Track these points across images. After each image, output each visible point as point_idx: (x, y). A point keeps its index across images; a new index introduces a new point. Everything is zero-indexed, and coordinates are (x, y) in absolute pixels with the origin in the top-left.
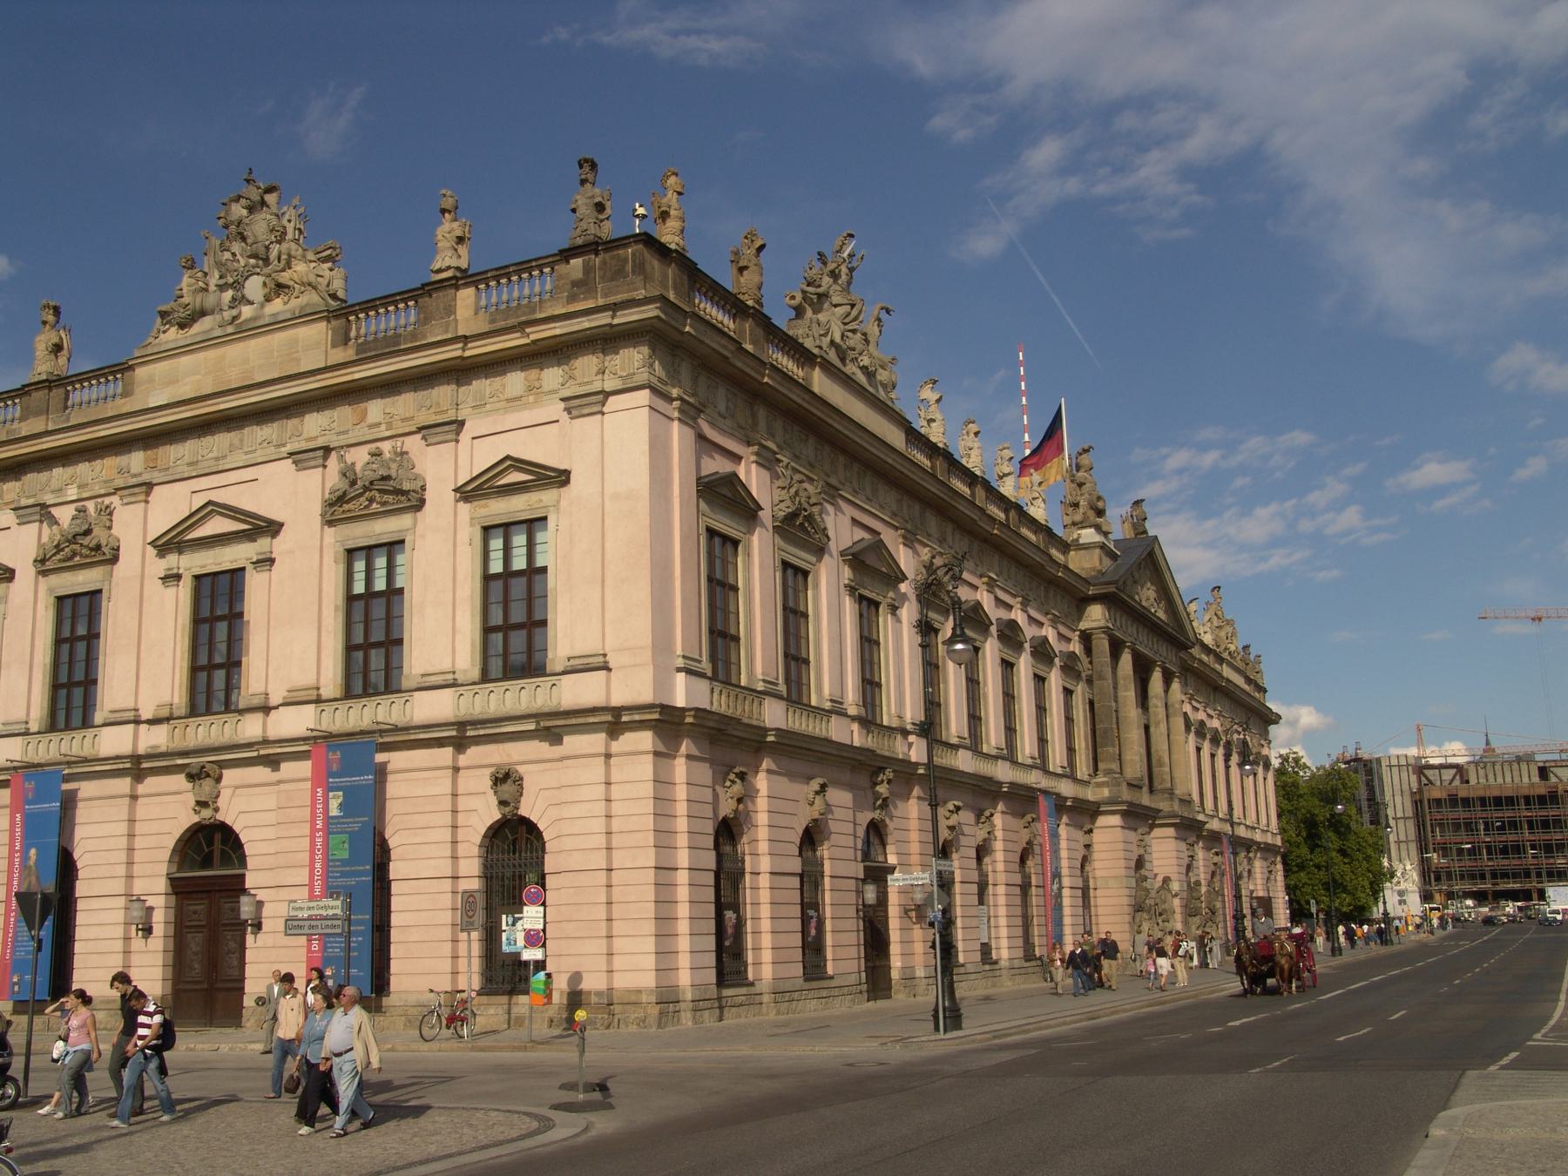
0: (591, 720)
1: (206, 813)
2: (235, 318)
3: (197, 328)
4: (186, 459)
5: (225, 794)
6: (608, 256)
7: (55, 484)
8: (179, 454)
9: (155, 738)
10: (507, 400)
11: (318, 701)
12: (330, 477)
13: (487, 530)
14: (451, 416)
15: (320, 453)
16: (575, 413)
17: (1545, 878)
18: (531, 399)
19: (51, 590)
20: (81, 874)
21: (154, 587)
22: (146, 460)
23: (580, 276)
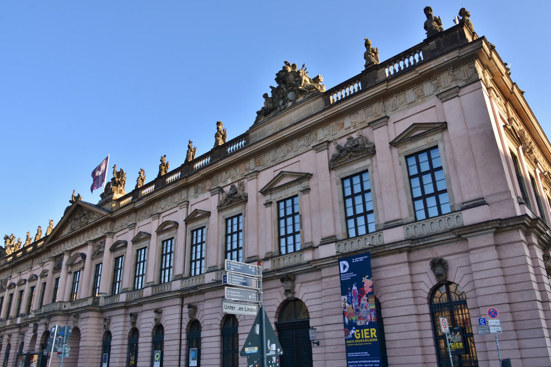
1: (290, 295)
2: (285, 107)
4: (271, 160)
5: (298, 286)
10: (408, 104)
11: (336, 241)
13: (407, 157)
14: (383, 115)
15: (326, 144)
18: (420, 100)
19: (223, 217)
20: (240, 324)
21: (262, 208)
22: (255, 163)
23: (435, 47)
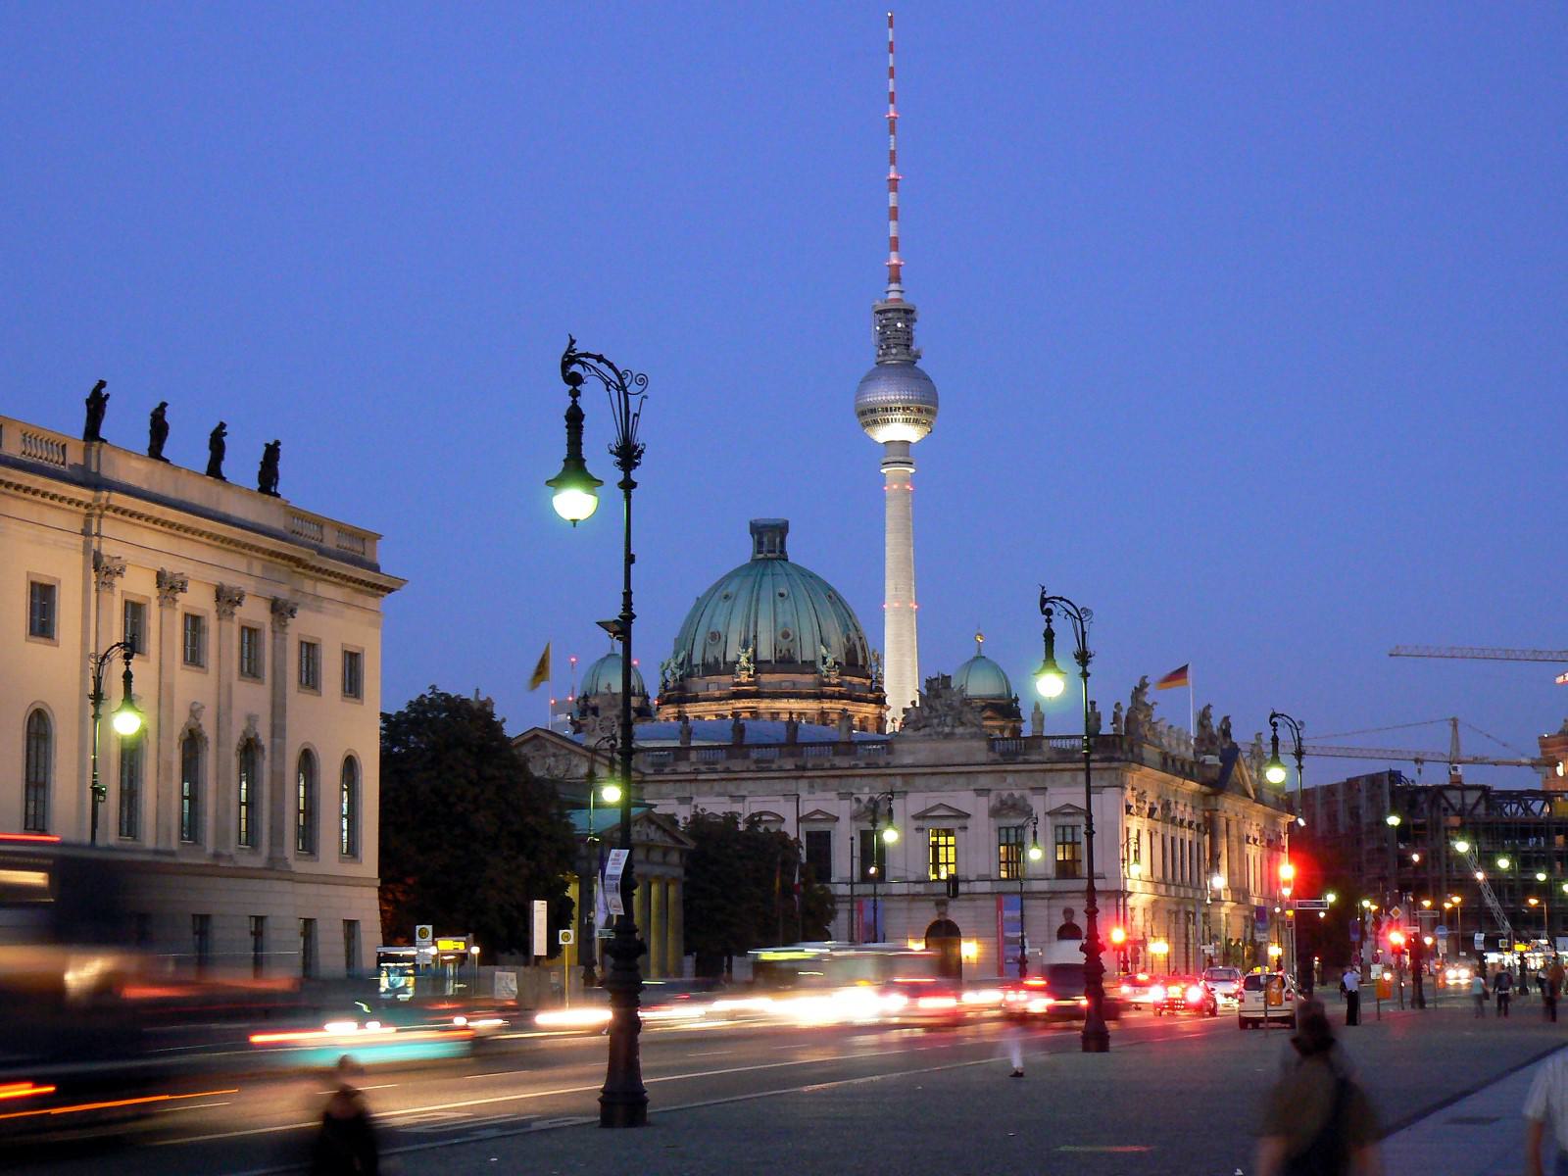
3: (922, 732)
8: (920, 782)
12: (992, 800)
13: (1057, 827)
17: (1518, 885)
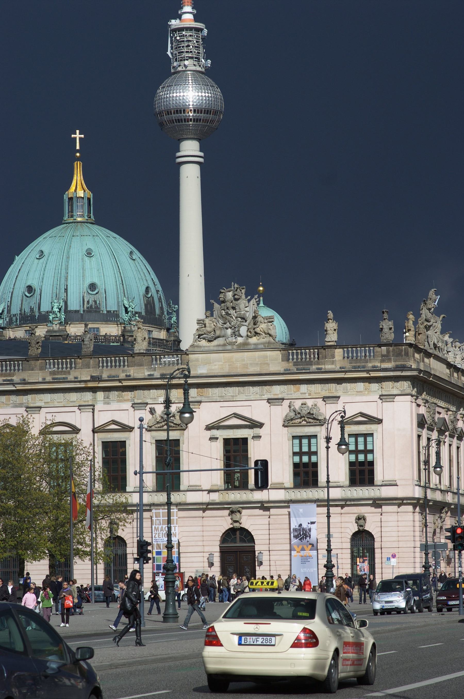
0: (394, 502)
3: (215, 343)
6: (395, 348)
7: (152, 396)
9: (215, 497)
16: (384, 400)
18: (366, 392)
